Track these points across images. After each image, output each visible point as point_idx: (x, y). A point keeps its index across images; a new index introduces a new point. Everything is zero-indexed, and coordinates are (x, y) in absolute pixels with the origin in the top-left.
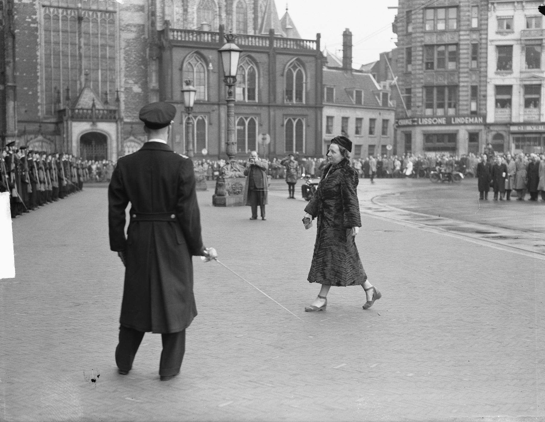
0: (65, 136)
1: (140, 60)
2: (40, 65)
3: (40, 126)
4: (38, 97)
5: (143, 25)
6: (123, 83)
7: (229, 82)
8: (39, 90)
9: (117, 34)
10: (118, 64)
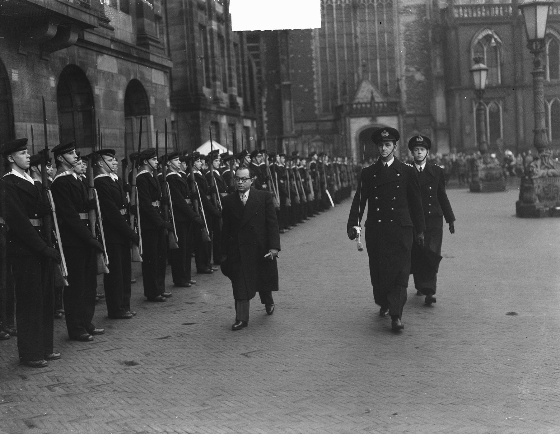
0: (343, 133)
1: (422, 44)
2: (315, 60)
3: (317, 125)
4: (314, 94)
5: (424, 5)
6: (404, 71)
7: (534, 47)
8: (315, 87)
9: (395, 19)
10: (398, 52)
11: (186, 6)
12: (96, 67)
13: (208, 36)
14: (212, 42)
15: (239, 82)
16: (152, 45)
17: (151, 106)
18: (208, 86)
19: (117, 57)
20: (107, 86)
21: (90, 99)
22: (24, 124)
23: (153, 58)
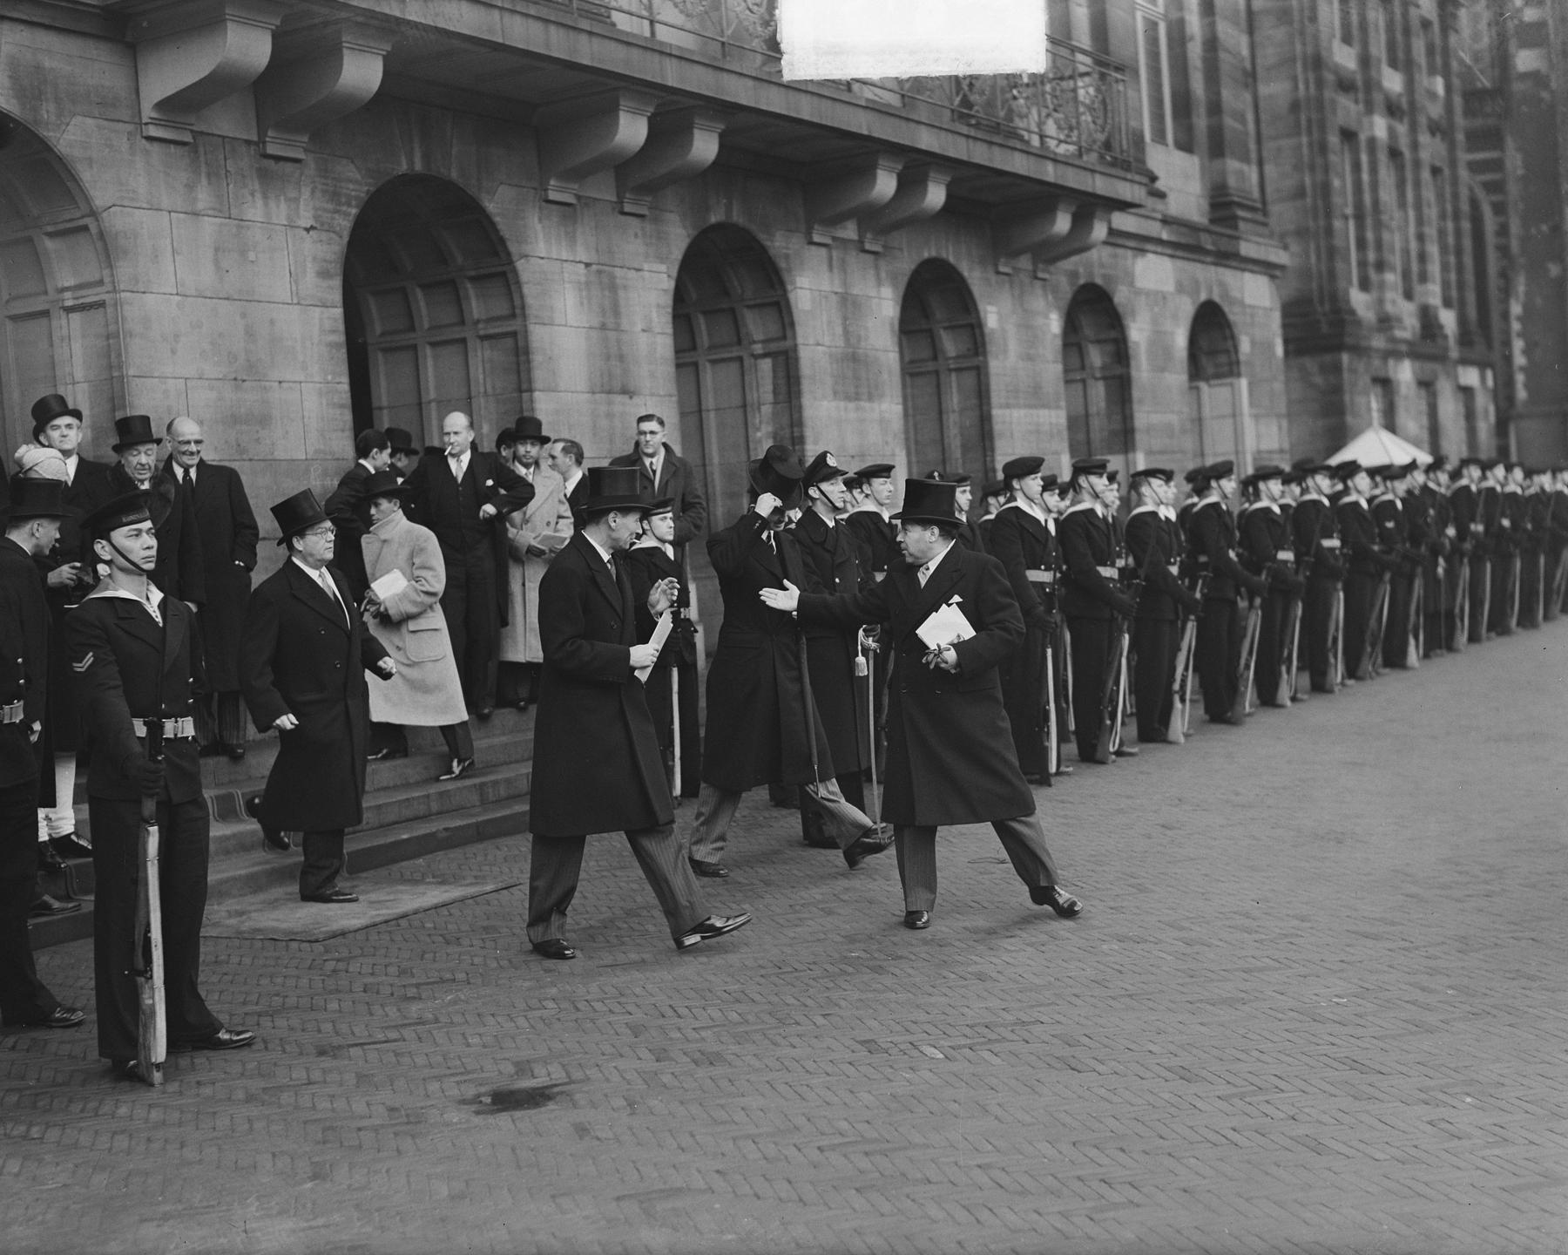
11: (1307, 88)
12: (1132, 284)
13: (1364, 158)
14: (1374, 170)
15: (1445, 267)
16: (1244, 219)
17: (1242, 358)
18: (1365, 285)
19: (1172, 256)
20: (1155, 321)
21: (1121, 352)
22: (1007, 412)
23: (1247, 249)
